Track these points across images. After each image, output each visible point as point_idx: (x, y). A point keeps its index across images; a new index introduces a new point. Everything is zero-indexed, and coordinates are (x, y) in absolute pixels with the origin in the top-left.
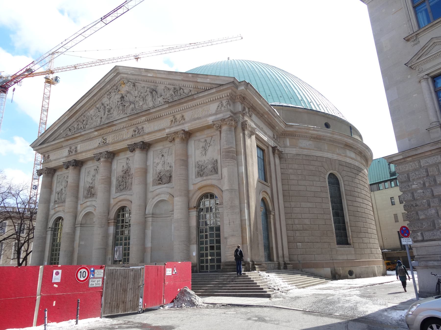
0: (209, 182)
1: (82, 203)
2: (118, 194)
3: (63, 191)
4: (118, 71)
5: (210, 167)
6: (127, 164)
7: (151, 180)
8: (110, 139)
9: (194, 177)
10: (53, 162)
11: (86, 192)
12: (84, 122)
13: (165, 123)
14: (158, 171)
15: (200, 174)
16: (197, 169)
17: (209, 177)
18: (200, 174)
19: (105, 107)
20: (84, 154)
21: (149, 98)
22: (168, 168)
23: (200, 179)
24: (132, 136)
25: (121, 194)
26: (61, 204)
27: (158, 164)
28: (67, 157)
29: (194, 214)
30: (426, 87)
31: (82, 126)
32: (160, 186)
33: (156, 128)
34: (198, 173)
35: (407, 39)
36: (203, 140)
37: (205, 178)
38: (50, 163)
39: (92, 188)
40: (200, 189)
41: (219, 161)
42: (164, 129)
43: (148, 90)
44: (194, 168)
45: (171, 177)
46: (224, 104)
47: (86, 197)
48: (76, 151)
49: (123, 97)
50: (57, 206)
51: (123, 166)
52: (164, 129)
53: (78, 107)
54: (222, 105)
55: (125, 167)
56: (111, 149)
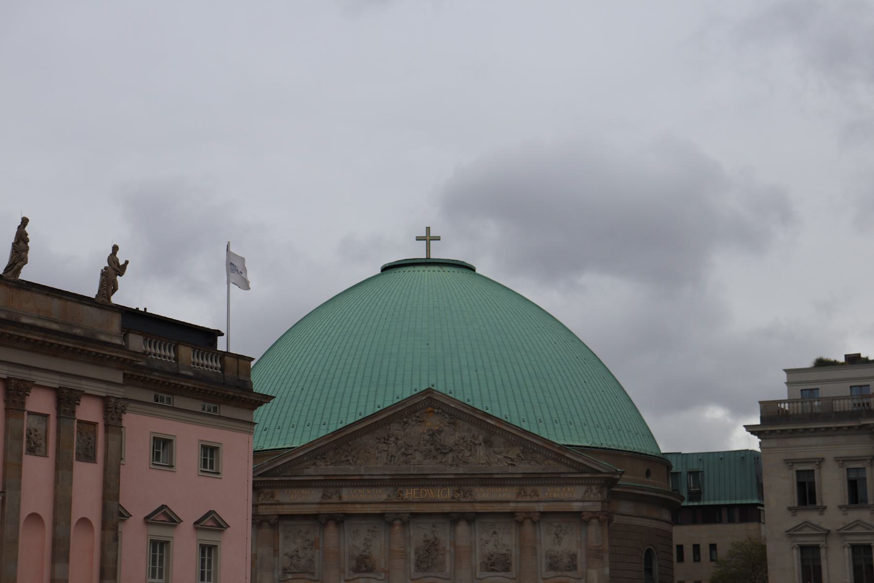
1: (347, 578)
2: (421, 575)
3: (301, 554)
4: (429, 395)
6: (433, 532)
7: (478, 562)
8: (410, 493)
9: (544, 569)
10: (286, 507)
11: (354, 563)
12: (354, 453)
13: (507, 493)
16: (549, 560)
19: (397, 439)
20: (358, 506)
21: (481, 451)
22: (504, 551)
23: (552, 574)
24: (453, 498)
25: (425, 574)
26: (300, 576)
27: (487, 542)
28: (320, 503)
30: (796, 553)
31: (349, 458)
32: (492, 574)
33: (494, 497)
35: (790, 509)
37: (559, 573)
38: (278, 507)
39: (366, 557)
41: (579, 556)
42: (508, 502)
43: (481, 438)
45: (510, 564)
46: (595, 491)
47: (357, 570)
48: (340, 497)
49: (432, 435)
50: (290, 576)
51: (425, 535)
52: (508, 502)
53: (349, 431)
54: (592, 491)
55: (430, 537)
56: (414, 508)
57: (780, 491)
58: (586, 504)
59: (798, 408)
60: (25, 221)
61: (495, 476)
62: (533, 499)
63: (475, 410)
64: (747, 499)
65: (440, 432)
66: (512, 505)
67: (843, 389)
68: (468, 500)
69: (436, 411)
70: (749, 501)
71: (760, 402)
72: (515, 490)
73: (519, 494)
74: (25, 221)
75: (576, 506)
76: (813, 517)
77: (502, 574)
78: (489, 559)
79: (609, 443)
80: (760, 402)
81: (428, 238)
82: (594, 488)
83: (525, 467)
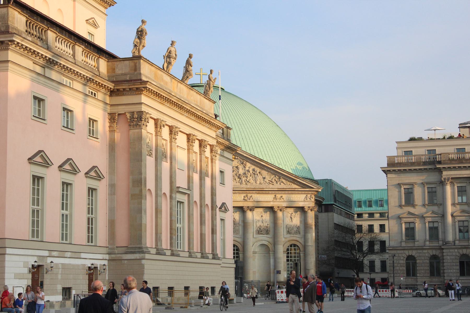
0: (295, 238)
5: (295, 229)
7: (255, 230)
9: (285, 233)
14: (258, 225)
15: (289, 232)
17: (295, 235)
18: (289, 232)
22: (266, 225)
23: (289, 235)
24: (244, 199)
29: (286, 255)
34: (288, 231)
36: (291, 213)
37: (292, 235)
40: (289, 241)
44: (285, 229)
57: (395, 198)
58: (306, 203)
59: (404, 160)
60: (190, 56)
61: (265, 189)
62: (281, 200)
63: (255, 157)
64: (328, 202)
65: (237, 167)
66: (272, 203)
67: (451, 150)
68: (251, 200)
69: (236, 157)
70: (329, 203)
71: (387, 157)
72: (273, 196)
73: (275, 198)
74: (190, 56)
75: (301, 204)
76: (411, 210)
77: (265, 235)
78: (260, 229)
79: (299, 174)
80: (387, 157)
81: (201, 74)
82: (309, 195)
83: (277, 186)
